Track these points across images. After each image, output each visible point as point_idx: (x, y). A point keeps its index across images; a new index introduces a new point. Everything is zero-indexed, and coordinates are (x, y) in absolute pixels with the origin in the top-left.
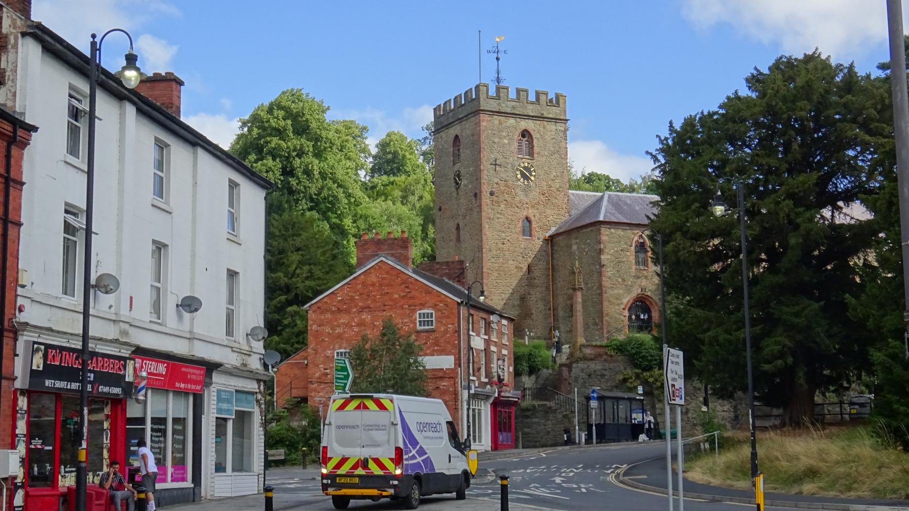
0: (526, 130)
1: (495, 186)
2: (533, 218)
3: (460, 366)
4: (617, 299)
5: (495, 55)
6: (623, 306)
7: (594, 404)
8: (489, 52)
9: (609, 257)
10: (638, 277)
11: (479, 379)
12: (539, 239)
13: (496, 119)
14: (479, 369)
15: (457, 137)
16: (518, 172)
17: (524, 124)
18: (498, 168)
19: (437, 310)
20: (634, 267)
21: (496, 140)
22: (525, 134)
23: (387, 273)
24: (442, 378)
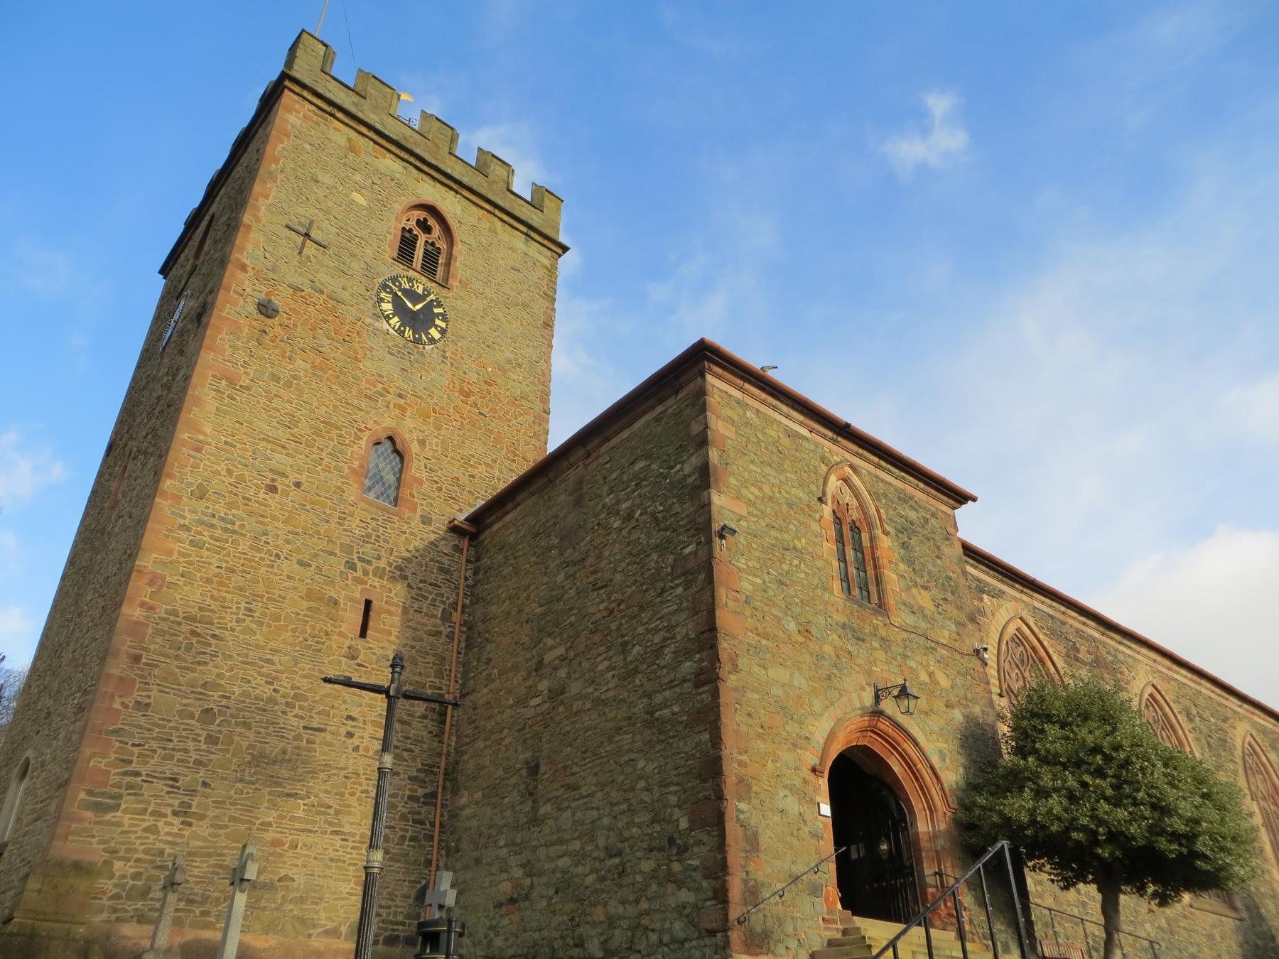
2: (415, 447)
12: (426, 521)
13: (340, 134)
18: (310, 249)
21: (326, 179)
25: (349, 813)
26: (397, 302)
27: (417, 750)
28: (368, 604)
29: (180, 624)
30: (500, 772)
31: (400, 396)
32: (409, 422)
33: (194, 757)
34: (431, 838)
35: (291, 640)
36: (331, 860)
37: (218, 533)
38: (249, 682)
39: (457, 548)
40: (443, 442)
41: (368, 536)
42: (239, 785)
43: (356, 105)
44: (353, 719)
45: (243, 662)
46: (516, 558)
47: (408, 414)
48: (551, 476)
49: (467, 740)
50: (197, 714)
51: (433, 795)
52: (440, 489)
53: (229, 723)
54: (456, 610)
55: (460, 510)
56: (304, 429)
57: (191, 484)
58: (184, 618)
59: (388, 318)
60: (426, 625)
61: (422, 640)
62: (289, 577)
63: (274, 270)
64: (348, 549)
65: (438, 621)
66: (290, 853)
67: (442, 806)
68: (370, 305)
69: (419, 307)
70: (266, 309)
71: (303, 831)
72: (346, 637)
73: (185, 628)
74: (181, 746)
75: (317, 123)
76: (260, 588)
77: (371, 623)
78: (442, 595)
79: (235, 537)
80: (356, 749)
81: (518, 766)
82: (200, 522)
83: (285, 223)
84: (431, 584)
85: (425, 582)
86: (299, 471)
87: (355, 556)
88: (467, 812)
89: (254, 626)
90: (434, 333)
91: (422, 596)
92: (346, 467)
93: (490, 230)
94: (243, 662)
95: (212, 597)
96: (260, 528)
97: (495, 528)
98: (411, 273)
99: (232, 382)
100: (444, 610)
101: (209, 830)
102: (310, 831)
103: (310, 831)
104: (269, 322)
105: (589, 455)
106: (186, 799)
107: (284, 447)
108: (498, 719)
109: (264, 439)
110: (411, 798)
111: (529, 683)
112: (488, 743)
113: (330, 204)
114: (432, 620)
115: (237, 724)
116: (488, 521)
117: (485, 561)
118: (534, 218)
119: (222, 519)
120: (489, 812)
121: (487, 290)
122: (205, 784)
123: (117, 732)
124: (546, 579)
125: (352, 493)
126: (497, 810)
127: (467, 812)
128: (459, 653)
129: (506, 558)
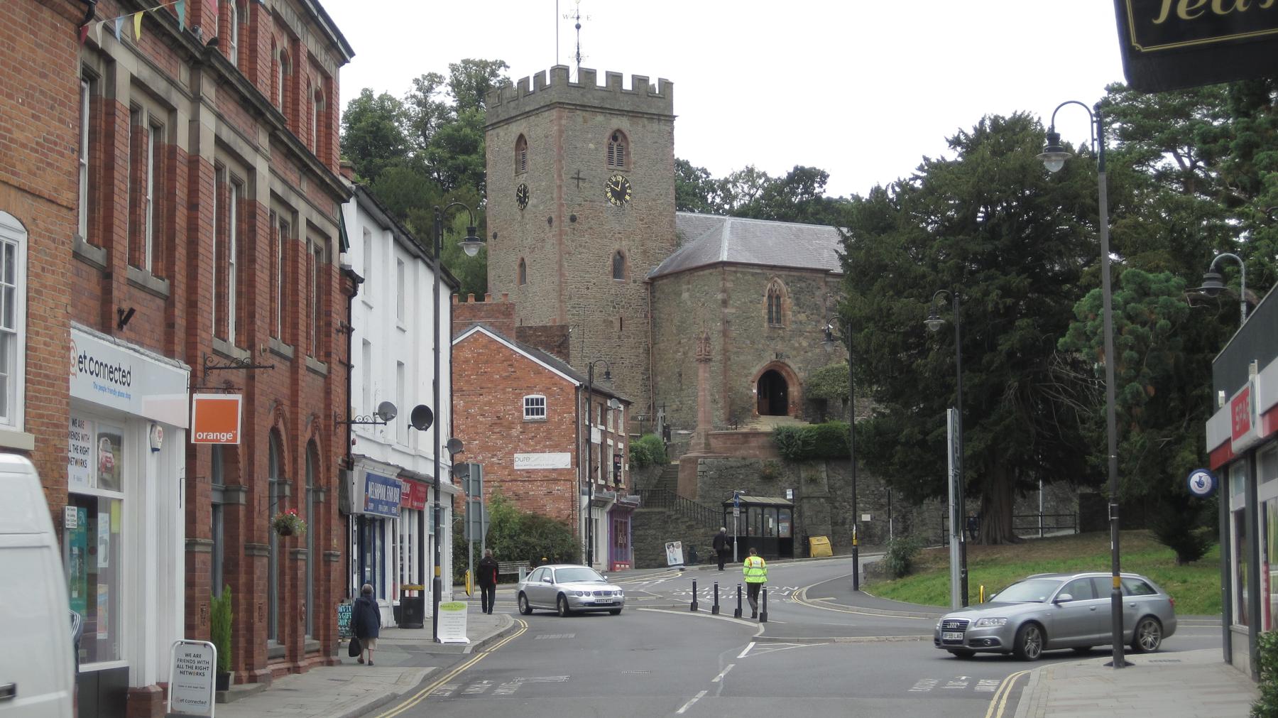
0: (618, 130)
1: (577, 208)
3: (578, 465)
4: (744, 368)
5: (575, 22)
6: (751, 378)
7: (736, 511)
8: (566, 17)
9: (733, 311)
10: (771, 338)
11: (596, 481)
12: (635, 282)
14: (596, 470)
15: (521, 137)
16: (608, 190)
19: (550, 395)
20: (766, 325)
23: (485, 347)
24: (556, 480)
26: (613, 191)
70: (573, 219)
90: (627, 197)
117: (657, 295)
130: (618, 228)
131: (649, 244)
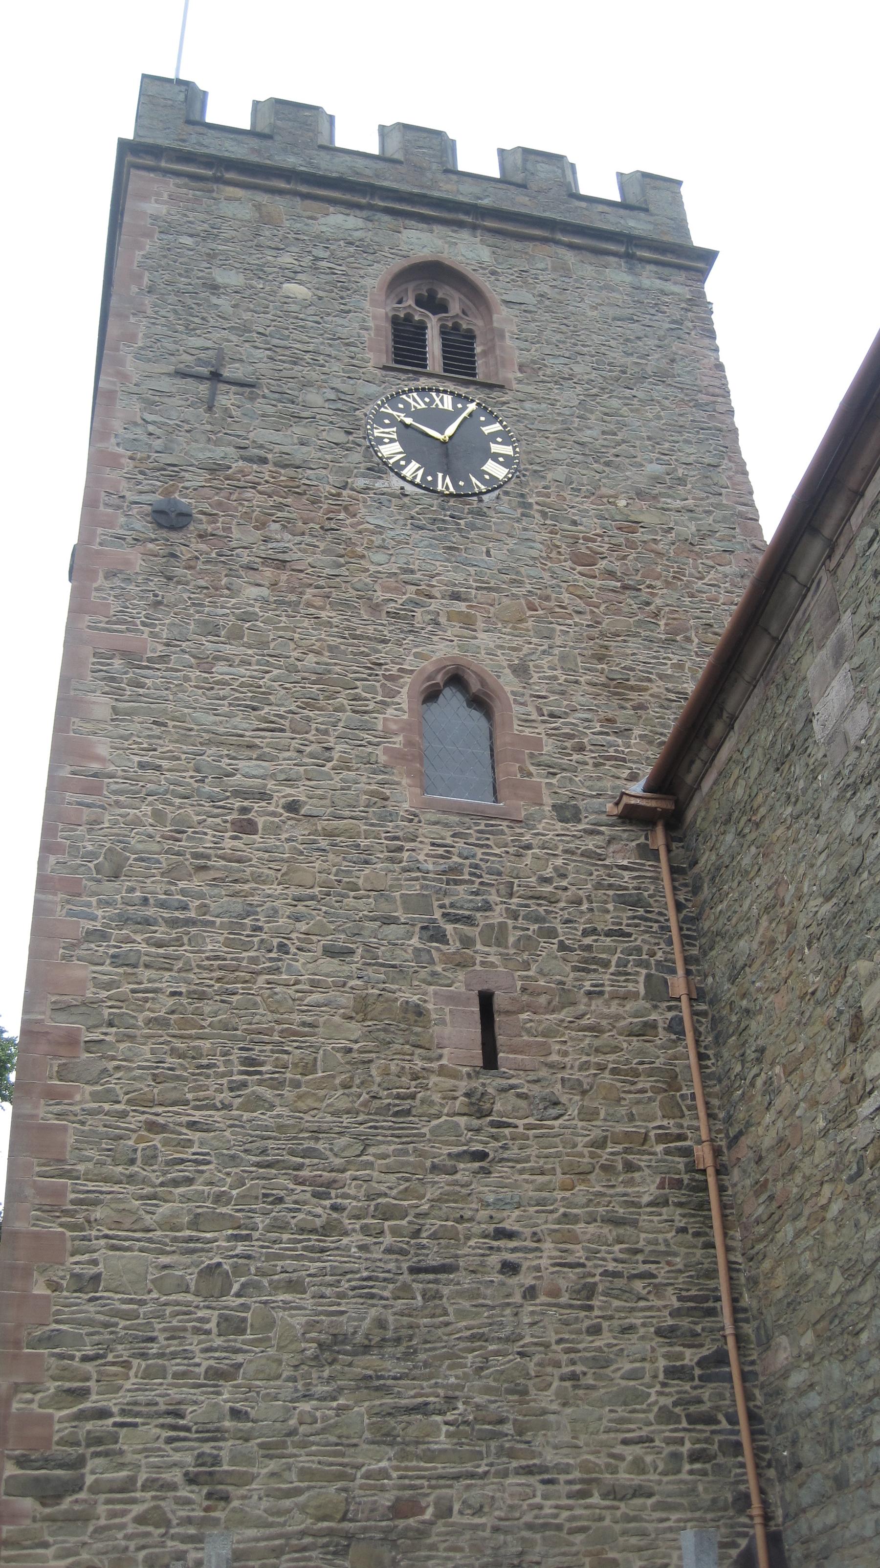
1: (196, 479)
2: (508, 683)
12: (567, 812)
17: (422, 243)
18: (227, 398)
21: (231, 278)
22: (431, 281)
25: (546, 1426)
27: (662, 1272)
28: (486, 1000)
29: (123, 1115)
30: (837, 1281)
31: (456, 597)
32: (484, 639)
33: (205, 1364)
34: (737, 1447)
35: (343, 1104)
36: (530, 1527)
37: (161, 932)
38: (280, 1200)
39: (647, 852)
40: (563, 658)
41: (455, 869)
42: (305, 1406)
43: (258, 152)
44: (510, 1235)
45: (258, 1165)
46: (757, 825)
47: (480, 625)
48: (774, 628)
49: (761, 1229)
50: (192, 1279)
51: (721, 1358)
52: (580, 749)
53: (257, 1286)
54: (673, 971)
55: (633, 778)
56: (282, 704)
57: (93, 855)
58: (129, 1102)
59: (396, 470)
60: (618, 1017)
61: (616, 1049)
62: (314, 984)
63: (166, 450)
64: (420, 903)
65: (642, 1004)
66: (440, 1528)
67: (745, 1377)
68: (356, 457)
69: (450, 430)
71: (457, 1477)
72: (455, 1075)
73: (135, 1120)
74: (174, 1346)
75: (197, 200)
76: (263, 1017)
77: (501, 1039)
78: (638, 950)
79: (193, 930)
80: (530, 1293)
81: (869, 1257)
82: (124, 920)
83: (171, 368)
84: (608, 934)
85: (594, 931)
86: (289, 781)
87: (437, 915)
88: (796, 1379)
89: (267, 1093)
91: (595, 961)
92: (379, 751)
93: (554, 269)
94: (258, 1165)
95: (174, 1052)
96: (237, 905)
97: (706, 785)
98: (423, 382)
99: (130, 657)
100: (649, 977)
101: (265, 1504)
102: (472, 1476)
103: (472, 1476)
104: (174, 536)
105: (831, 546)
106: (207, 1448)
107: (250, 747)
108: (806, 1167)
109: (209, 743)
110: (674, 1373)
111: (846, 1071)
112: (801, 1223)
113: (247, 316)
114: (630, 1006)
115: (276, 1287)
116: (690, 779)
117: (707, 859)
118: (636, 224)
119: (162, 905)
120: (836, 1369)
121: (578, 369)
122: (236, 1414)
123: (49, 1340)
124: (822, 840)
125: (405, 796)
126: (850, 1364)
127: (796, 1379)
128: (701, 1057)
129: (740, 834)
130: (450, 575)
131: (633, 653)
